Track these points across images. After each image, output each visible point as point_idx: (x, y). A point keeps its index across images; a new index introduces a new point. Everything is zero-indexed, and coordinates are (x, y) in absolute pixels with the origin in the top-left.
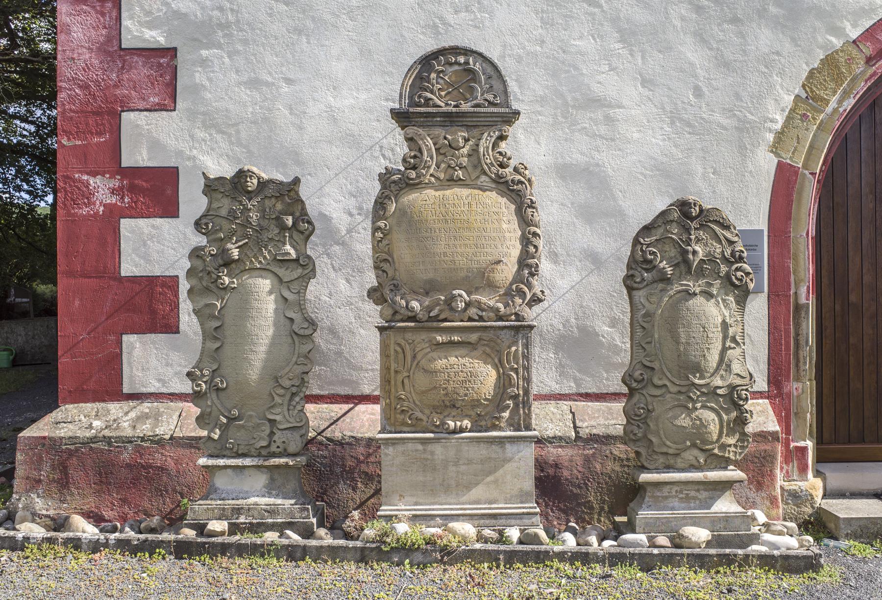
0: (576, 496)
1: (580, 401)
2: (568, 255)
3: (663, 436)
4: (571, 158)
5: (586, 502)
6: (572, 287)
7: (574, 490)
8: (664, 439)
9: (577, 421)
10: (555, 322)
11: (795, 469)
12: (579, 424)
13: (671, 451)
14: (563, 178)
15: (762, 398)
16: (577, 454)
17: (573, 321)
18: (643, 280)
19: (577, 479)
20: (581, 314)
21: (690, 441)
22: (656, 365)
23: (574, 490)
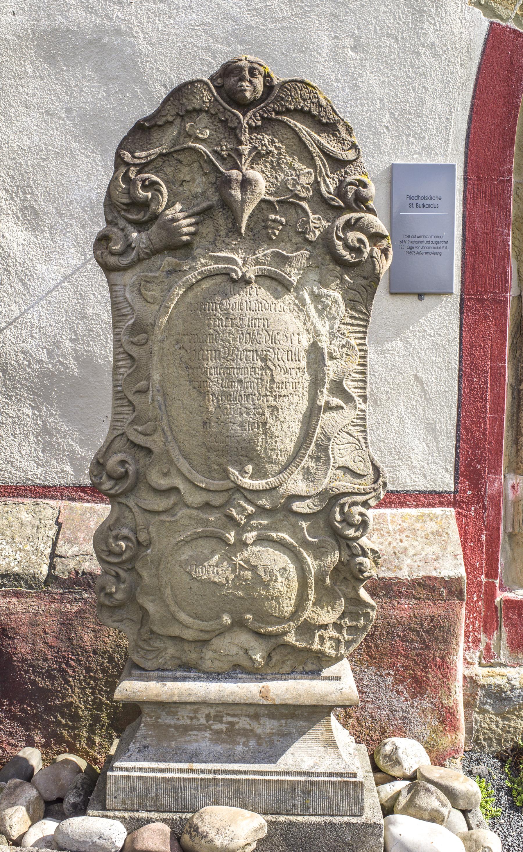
0: (44, 694)
1: (82, 500)
2: (60, 214)
3: (170, 601)
4: (66, 17)
5: (63, 706)
6: (67, 278)
7: (39, 680)
8: (174, 608)
9: (60, 542)
10: (32, 346)
11: (504, 643)
12: (61, 549)
13: (188, 634)
14: (51, 59)
15: (441, 504)
16: (47, 612)
17: (68, 344)
18: (129, 247)
19: (45, 660)
20: (82, 332)
21: (231, 613)
22: (155, 443)
23: (39, 680)
